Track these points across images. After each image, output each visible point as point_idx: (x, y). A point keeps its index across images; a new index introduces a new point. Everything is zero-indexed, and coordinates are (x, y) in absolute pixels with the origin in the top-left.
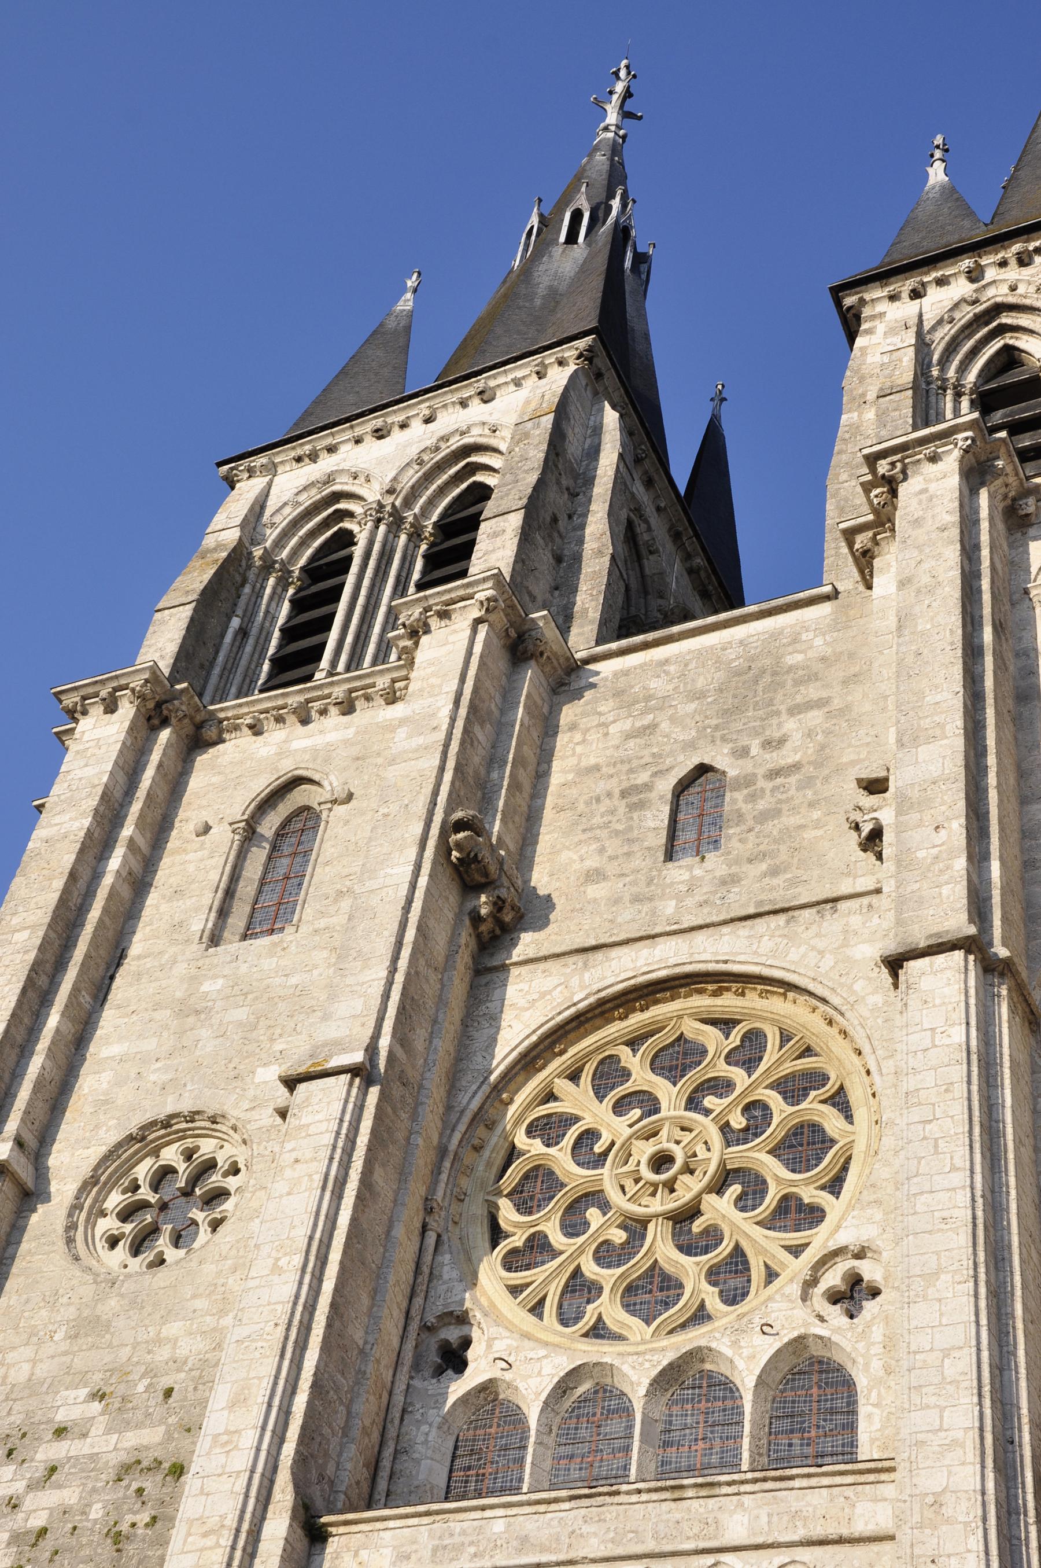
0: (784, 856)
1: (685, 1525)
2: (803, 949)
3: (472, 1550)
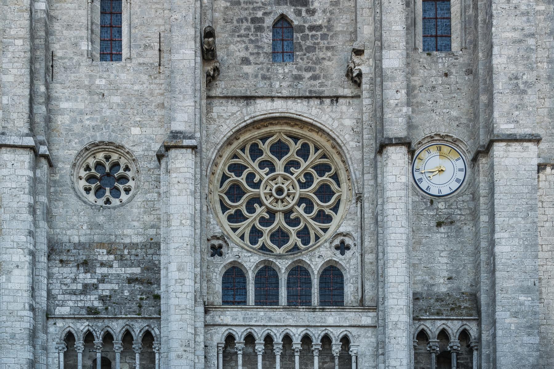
0: (317, 72)
1: (316, 318)
2: (327, 116)
3: (255, 319)
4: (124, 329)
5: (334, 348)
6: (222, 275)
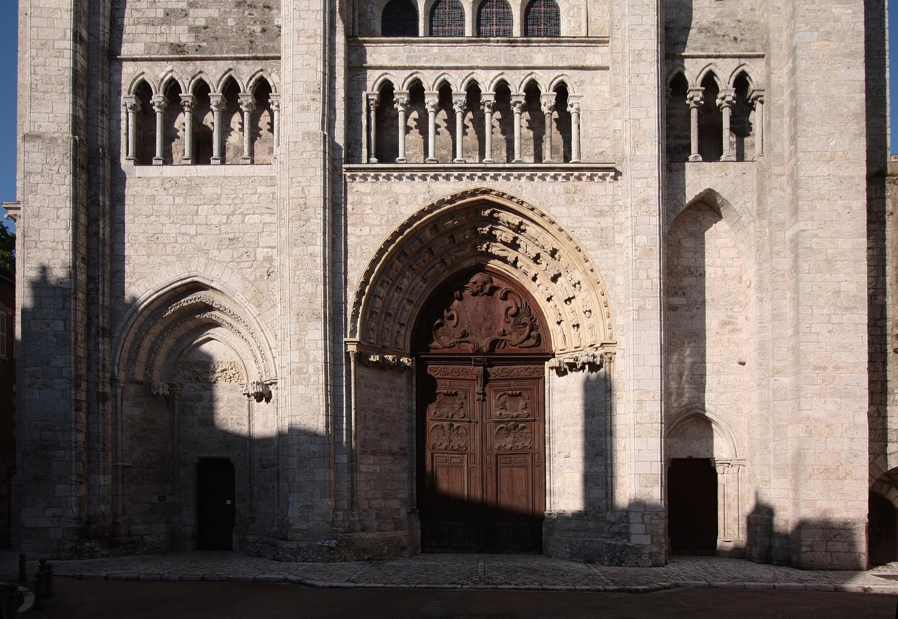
3: (425, 59)
4: (227, 76)
5: (543, 100)
6: (382, 9)
